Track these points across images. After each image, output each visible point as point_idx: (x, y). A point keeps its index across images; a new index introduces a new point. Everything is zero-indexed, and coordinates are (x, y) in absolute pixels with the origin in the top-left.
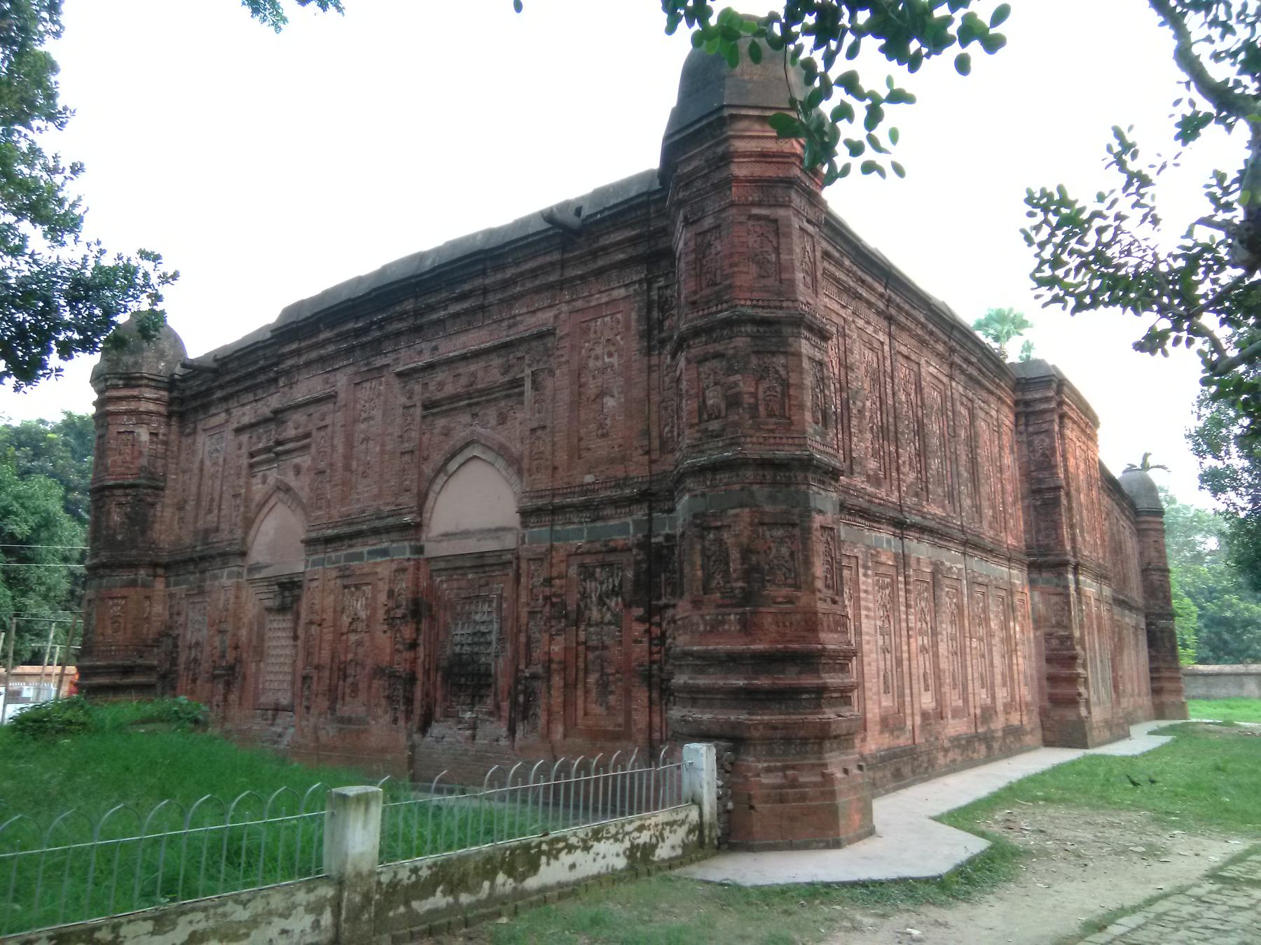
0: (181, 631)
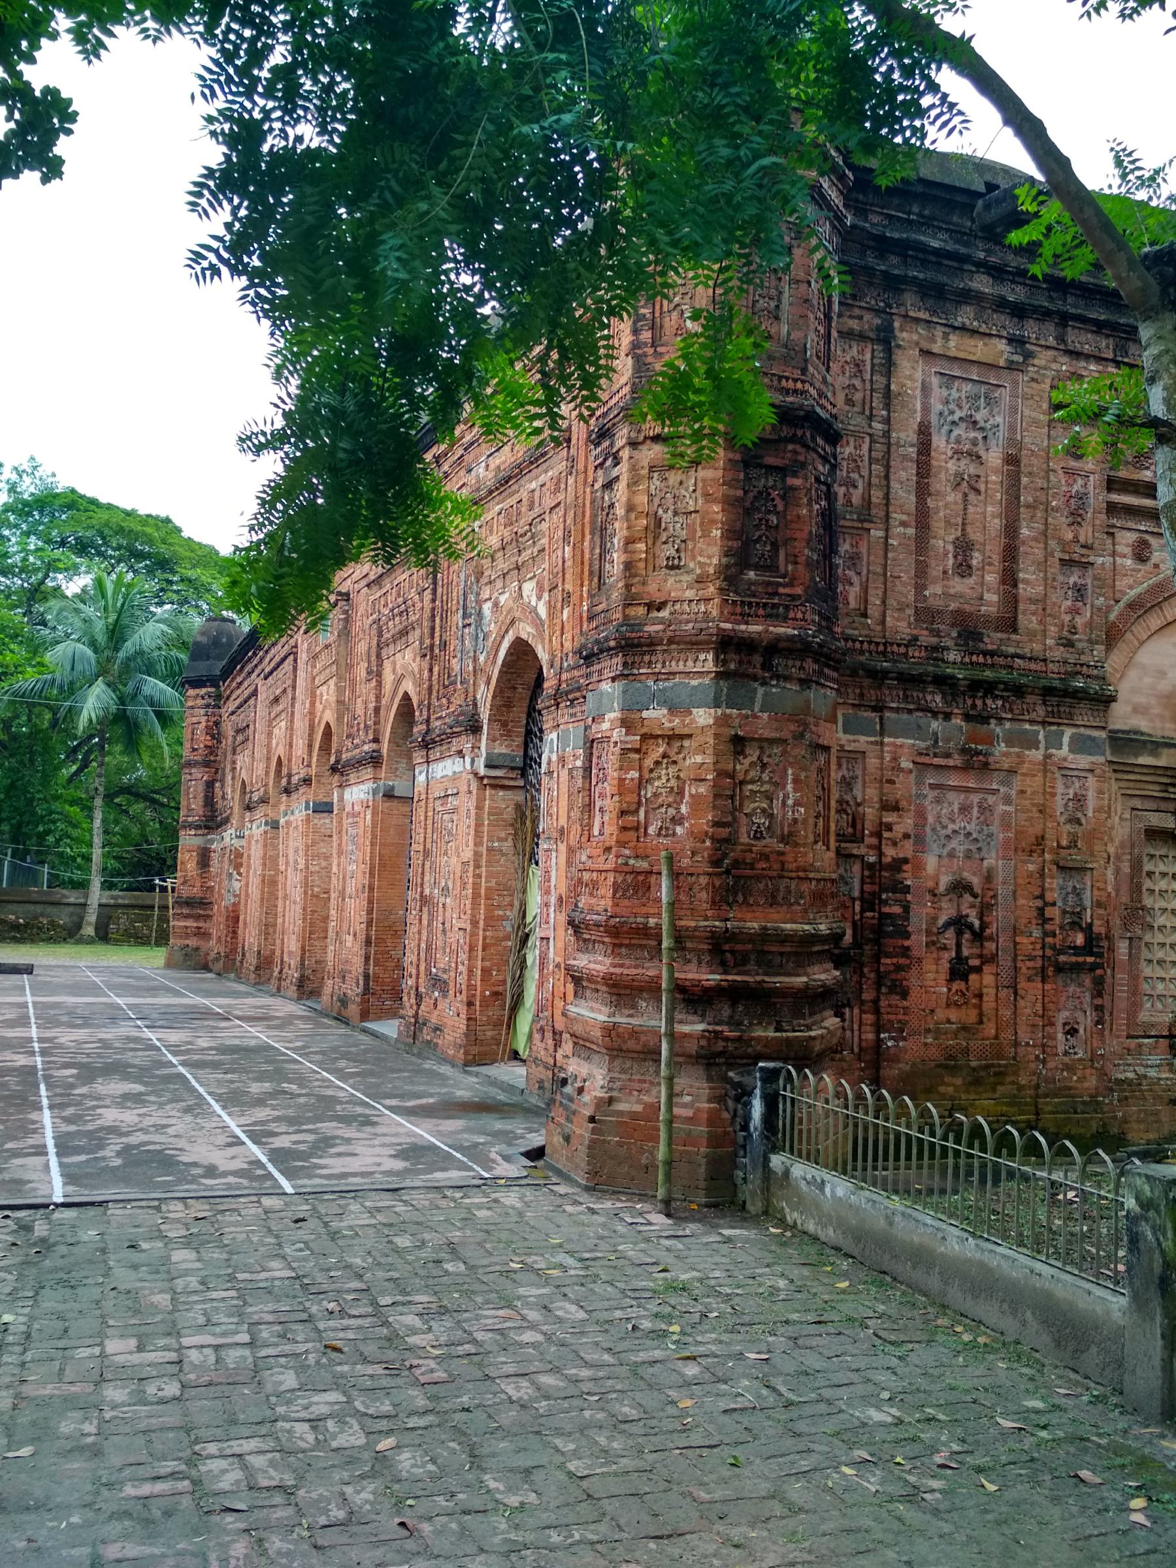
0: (907, 849)
